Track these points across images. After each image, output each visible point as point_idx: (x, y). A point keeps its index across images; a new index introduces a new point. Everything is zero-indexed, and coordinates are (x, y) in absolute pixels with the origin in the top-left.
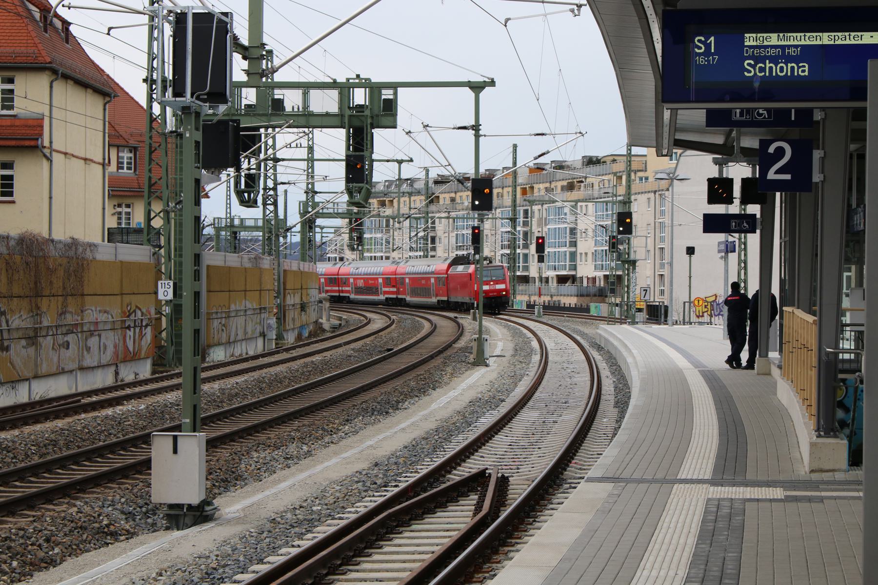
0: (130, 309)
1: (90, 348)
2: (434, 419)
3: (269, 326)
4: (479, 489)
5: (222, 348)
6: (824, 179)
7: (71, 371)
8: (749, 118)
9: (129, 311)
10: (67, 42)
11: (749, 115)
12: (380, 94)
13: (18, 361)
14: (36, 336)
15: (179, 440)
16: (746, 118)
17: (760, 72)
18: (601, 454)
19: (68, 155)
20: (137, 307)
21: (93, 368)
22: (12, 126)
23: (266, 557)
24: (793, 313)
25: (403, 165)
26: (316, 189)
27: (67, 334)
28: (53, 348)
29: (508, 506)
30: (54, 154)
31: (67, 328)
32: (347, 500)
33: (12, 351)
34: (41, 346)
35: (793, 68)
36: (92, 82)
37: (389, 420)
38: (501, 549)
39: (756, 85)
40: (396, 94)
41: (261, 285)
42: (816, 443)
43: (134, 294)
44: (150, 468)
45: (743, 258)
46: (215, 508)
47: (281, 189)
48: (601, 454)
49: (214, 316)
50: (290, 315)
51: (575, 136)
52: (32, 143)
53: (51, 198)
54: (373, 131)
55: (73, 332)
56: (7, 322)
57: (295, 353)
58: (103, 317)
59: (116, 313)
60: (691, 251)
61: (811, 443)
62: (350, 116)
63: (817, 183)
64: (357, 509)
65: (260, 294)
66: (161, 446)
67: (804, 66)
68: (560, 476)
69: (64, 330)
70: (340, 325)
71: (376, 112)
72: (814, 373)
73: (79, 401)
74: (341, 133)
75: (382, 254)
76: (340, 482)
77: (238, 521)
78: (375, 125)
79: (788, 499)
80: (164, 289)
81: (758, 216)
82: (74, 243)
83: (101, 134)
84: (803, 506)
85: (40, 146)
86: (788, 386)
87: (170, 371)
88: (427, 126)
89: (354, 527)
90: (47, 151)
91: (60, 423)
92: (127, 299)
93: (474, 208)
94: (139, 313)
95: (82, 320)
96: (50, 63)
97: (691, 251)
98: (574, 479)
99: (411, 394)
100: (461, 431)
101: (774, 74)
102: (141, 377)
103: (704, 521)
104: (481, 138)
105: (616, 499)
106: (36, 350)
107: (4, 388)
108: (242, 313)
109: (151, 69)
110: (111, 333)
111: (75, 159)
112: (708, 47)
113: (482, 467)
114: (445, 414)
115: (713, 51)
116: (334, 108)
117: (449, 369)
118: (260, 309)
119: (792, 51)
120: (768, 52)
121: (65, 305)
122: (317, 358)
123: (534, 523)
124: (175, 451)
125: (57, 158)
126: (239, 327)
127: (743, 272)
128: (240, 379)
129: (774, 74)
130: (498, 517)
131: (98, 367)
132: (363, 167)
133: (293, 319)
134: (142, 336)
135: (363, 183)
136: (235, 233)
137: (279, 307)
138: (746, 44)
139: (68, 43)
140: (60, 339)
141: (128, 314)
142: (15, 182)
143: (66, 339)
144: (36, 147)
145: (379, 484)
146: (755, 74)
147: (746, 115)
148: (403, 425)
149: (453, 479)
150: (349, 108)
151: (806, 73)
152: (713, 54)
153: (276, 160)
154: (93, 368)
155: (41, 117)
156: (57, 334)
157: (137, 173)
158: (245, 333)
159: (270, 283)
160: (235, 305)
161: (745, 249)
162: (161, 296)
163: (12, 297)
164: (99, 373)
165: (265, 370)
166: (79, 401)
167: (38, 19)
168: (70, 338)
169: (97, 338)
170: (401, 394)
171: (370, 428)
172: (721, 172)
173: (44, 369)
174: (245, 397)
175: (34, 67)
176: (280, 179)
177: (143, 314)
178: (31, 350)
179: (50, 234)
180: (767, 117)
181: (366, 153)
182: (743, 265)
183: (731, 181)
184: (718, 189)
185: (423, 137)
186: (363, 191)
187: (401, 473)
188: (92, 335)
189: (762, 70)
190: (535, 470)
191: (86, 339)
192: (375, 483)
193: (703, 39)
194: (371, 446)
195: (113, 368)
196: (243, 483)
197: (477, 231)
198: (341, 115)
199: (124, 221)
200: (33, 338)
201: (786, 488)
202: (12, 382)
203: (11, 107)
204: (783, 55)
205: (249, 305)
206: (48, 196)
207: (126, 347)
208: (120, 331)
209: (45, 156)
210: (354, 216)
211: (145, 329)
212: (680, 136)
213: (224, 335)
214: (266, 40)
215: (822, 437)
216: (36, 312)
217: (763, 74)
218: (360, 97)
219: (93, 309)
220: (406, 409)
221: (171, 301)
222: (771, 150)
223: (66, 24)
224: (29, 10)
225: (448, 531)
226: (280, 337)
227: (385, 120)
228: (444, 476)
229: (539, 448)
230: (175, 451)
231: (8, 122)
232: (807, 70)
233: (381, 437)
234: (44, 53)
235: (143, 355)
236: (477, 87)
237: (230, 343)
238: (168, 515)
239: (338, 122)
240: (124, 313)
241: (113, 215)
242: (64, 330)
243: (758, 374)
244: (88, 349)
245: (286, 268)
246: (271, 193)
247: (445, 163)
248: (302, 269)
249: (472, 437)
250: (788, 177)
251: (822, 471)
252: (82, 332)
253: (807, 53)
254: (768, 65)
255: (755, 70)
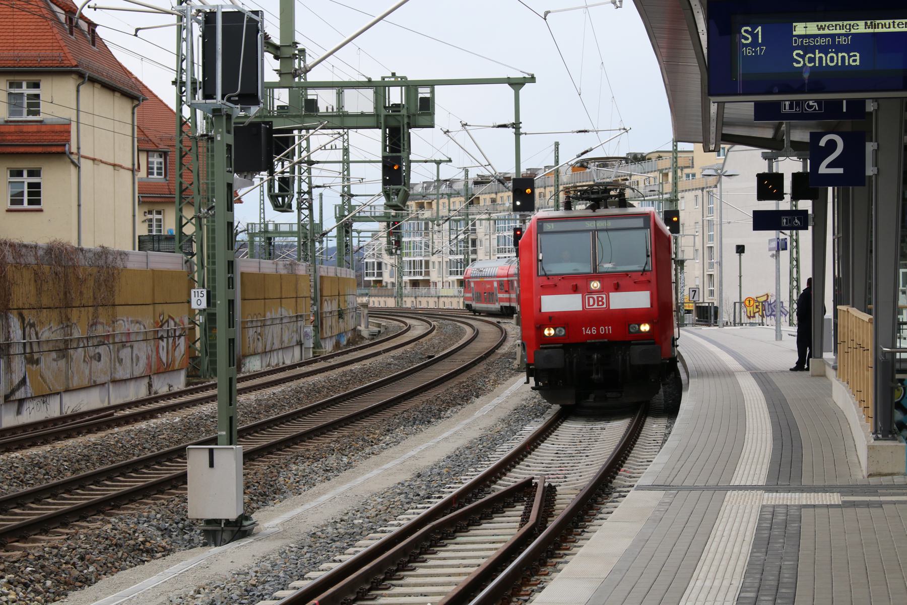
0: (163, 319)
1: (122, 359)
2: (477, 428)
3: (306, 335)
4: (525, 499)
5: (258, 357)
6: (878, 172)
7: (103, 384)
8: (799, 111)
9: (161, 321)
10: (94, 45)
11: (799, 108)
12: (417, 93)
13: (48, 375)
14: (67, 349)
15: (216, 453)
16: (796, 111)
17: (810, 62)
18: (651, 461)
19: (96, 162)
20: (170, 317)
21: (125, 380)
22: (38, 132)
23: (306, 573)
24: (848, 312)
25: (442, 165)
26: (352, 192)
27: (98, 345)
28: (84, 361)
29: (555, 517)
30: (82, 160)
31: (98, 339)
32: (389, 512)
33: (42, 364)
34: (72, 359)
35: (843, 57)
36: (120, 86)
37: (431, 430)
38: (549, 560)
39: (806, 75)
40: (433, 92)
41: (296, 292)
42: (873, 446)
43: (166, 303)
44: (186, 483)
45: (795, 256)
46: (254, 523)
47: (315, 192)
48: (651, 461)
49: (249, 325)
50: (327, 323)
51: (618, 133)
52: (59, 149)
53: (79, 206)
54: (410, 131)
55: (104, 344)
56: (37, 334)
57: (333, 362)
58: (135, 328)
59: (148, 324)
60: (740, 249)
61: (868, 446)
62: (386, 116)
63: (870, 177)
64: (400, 522)
65: (296, 301)
66: (196, 460)
67: (855, 56)
68: (609, 484)
69: (96, 341)
70: (379, 332)
71: (412, 111)
72: (870, 374)
73: (112, 414)
74: (377, 134)
75: (421, 258)
76: (382, 494)
77: (277, 535)
78: (411, 125)
79: (845, 505)
80: (197, 298)
81: (810, 212)
82: (104, 252)
83: (130, 138)
84: (862, 512)
85: (68, 152)
86: (844, 388)
87: (204, 382)
88: (466, 125)
89: (397, 541)
90: (74, 158)
91: (92, 438)
92: (159, 308)
93: (516, 209)
94: (172, 323)
95: (114, 331)
96: (76, 66)
97: (740, 249)
98: (624, 487)
99: (454, 402)
100: (506, 439)
101: (824, 65)
102: (175, 389)
103: (759, 529)
104: (521, 137)
105: (667, 507)
106: (67, 363)
107: (35, 402)
108: (278, 321)
109: (180, 71)
110: (144, 344)
111: (103, 165)
112: (755, 37)
113: (528, 477)
114: (489, 422)
115: (760, 41)
116: (369, 108)
117: (492, 377)
118: (297, 317)
119: (842, 40)
120: (817, 42)
121: (96, 316)
122: (356, 366)
123: (583, 533)
124: (211, 465)
125: (85, 164)
126: (275, 335)
127: (795, 270)
128: (277, 389)
129: (824, 65)
130: (546, 528)
131: (131, 379)
132: (400, 168)
133: (331, 327)
134: (175, 346)
135: (400, 184)
136: (270, 239)
137: (316, 314)
138: (794, 33)
139: (94, 45)
140: (92, 351)
141: (160, 324)
142: (42, 190)
143: (97, 351)
144: (64, 153)
145: (422, 495)
146: (805, 64)
147: (796, 108)
148: (446, 435)
149: (498, 490)
150: (385, 107)
151: (858, 63)
152: (760, 45)
153: (311, 163)
154: (125, 380)
155: (67, 122)
156: (88, 346)
157: (168, 178)
158: (282, 342)
159: (306, 290)
160: (271, 312)
161: (797, 247)
162: (194, 305)
163: (41, 308)
164: (132, 386)
165: (303, 380)
166: (112, 414)
167: (64, 22)
168: (102, 350)
169: (129, 349)
170: (444, 403)
171: (411, 438)
172: (770, 167)
173: (75, 383)
174: (282, 407)
175: (60, 71)
176: (314, 183)
177: (176, 324)
178: (62, 363)
179: (79, 243)
180: (817, 109)
181: (403, 154)
182: (795, 263)
183: (781, 176)
184: (768, 185)
185: (461, 136)
186: (401, 193)
187: (445, 484)
188: (124, 346)
189: (812, 60)
190: (583, 479)
191: (118, 351)
192: (418, 495)
193: (750, 29)
194: (414, 456)
195: (146, 381)
196: (282, 497)
197: (518, 233)
198: (376, 115)
199: (155, 228)
200: (63, 350)
201: (843, 494)
202: (43, 396)
203: (37, 113)
204: (832, 44)
205: (285, 313)
206: (76, 204)
207: (159, 359)
208: (152, 342)
209: (73, 162)
210: (391, 219)
211: (178, 339)
212: (727, 131)
213: (260, 344)
214: (297, 39)
215: (880, 440)
216: (66, 323)
217: (813, 64)
218: (396, 96)
219: (125, 319)
220: (448, 417)
221: (204, 310)
222: (822, 143)
223: (92, 26)
224: (54, 12)
225: (494, 543)
226: (317, 345)
227: (422, 120)
228: (489, 487)
229: (587, 456)
230: (211, 465)
231: (34, 128)
232: (858, 61)
233: (423, 447)
234: (70, 56)
235: (176, 367)
236: (517, 84)
237: (266, 352)
238: (205, 531)
239: (373, 123)
240: (156, 323)
241: (143, 222)
242: (96, 341)
243: (812, 376)
244: (121, 361)
245: (323, 274)
246: (306, 196)
247: (485, 163)
248: (339, 275)
249: (516, 444)
250: (840, 171)
251: (880, 475)
252: (114, 343)
253: (858, 42)
254: (818, 56)
255: (804, 60)
